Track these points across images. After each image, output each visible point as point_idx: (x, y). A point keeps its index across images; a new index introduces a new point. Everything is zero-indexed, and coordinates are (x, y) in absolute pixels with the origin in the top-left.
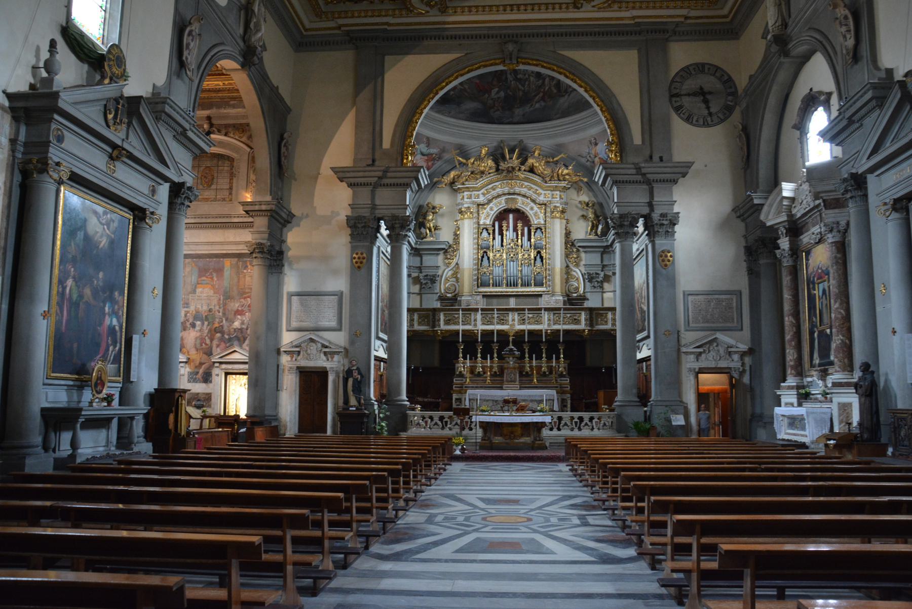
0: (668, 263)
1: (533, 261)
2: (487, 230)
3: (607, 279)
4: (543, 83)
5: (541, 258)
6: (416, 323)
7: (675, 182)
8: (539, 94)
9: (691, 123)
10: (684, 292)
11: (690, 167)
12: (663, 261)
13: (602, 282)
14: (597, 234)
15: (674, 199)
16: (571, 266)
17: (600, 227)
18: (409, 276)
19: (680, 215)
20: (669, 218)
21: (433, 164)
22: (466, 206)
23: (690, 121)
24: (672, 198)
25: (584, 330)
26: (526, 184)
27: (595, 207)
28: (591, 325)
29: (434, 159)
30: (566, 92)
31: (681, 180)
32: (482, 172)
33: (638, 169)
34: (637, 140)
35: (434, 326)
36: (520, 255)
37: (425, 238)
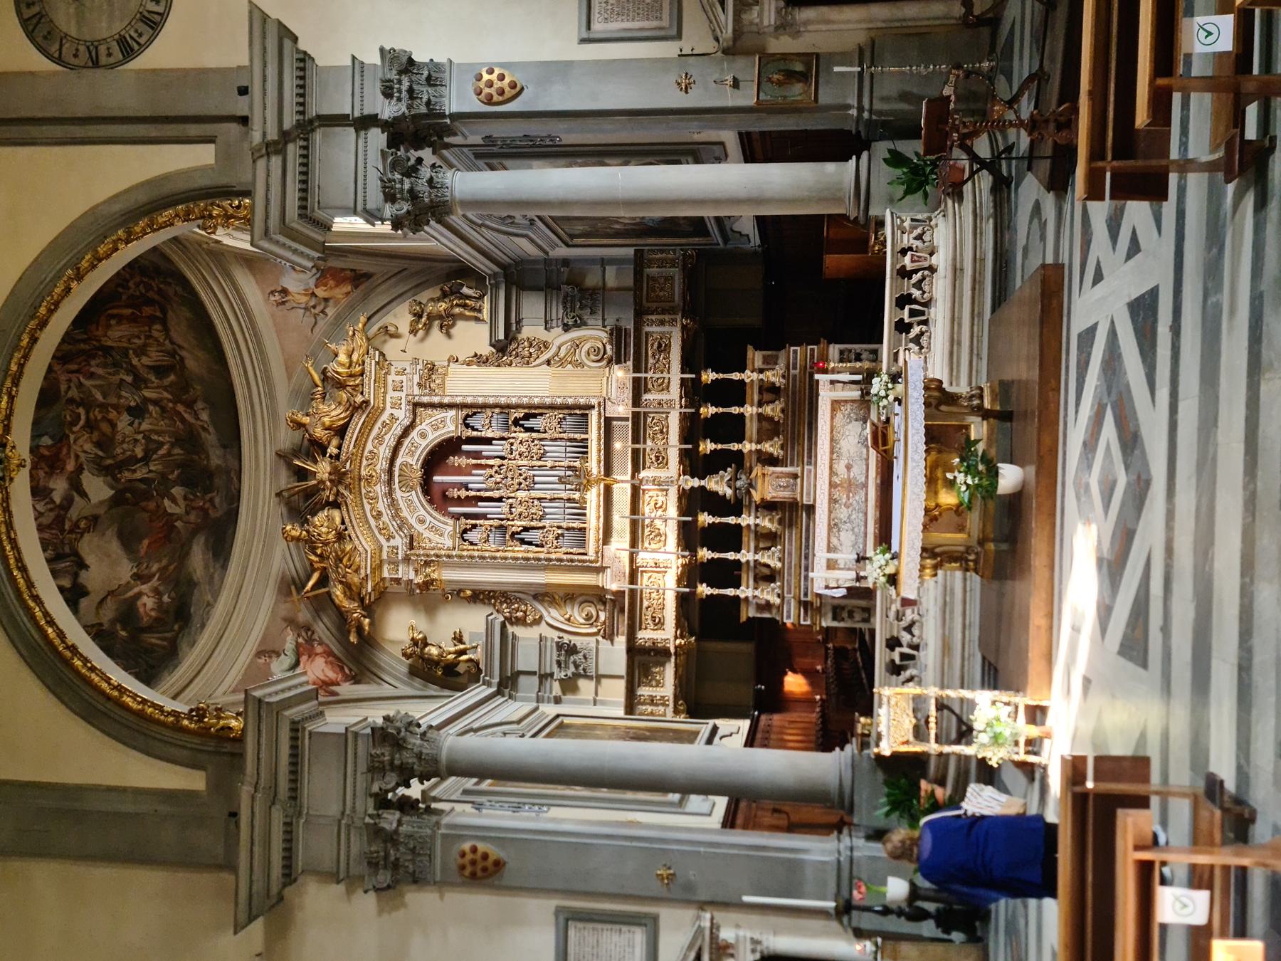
0: (507, 80)
1: (534, 435)
2: (465, 531)
3: (576, 282)
4: (156, 402)
5: (527, 417)
6: (658, 692)
7: (304, 59)
8: (179, 413)
9: (164, 16)
10: (583, 41)
11: (265, 18)
12: (501, 92)
13: (583, 290)
14: (481, 298)
15: (349, 63)
16: (544, 357)
17: (465, 290)
18: (557, 701)
19: (387, 47)
20: (393, 75)
21: (321, 643)
22: (412, 575)
23: (157, 18)
24: (345, 67)
25: (684, 327)
26: (369, 447)
27: (424, 301)
28: (671, 311)
29: (310, 641)
30: (172, 354)
31: (302, 45)
32: (340, 537)
33: (275, 148)
34: (203, 155)
35: (665, 653)
36: (520, 463)
37: (477, 663)
